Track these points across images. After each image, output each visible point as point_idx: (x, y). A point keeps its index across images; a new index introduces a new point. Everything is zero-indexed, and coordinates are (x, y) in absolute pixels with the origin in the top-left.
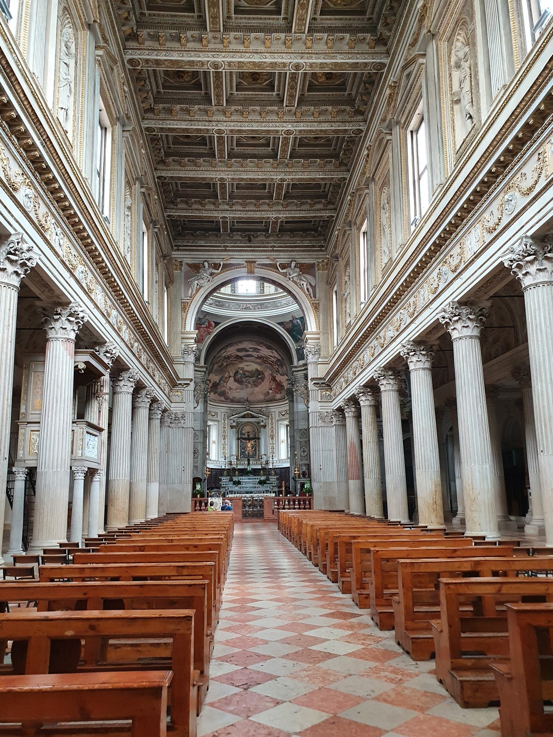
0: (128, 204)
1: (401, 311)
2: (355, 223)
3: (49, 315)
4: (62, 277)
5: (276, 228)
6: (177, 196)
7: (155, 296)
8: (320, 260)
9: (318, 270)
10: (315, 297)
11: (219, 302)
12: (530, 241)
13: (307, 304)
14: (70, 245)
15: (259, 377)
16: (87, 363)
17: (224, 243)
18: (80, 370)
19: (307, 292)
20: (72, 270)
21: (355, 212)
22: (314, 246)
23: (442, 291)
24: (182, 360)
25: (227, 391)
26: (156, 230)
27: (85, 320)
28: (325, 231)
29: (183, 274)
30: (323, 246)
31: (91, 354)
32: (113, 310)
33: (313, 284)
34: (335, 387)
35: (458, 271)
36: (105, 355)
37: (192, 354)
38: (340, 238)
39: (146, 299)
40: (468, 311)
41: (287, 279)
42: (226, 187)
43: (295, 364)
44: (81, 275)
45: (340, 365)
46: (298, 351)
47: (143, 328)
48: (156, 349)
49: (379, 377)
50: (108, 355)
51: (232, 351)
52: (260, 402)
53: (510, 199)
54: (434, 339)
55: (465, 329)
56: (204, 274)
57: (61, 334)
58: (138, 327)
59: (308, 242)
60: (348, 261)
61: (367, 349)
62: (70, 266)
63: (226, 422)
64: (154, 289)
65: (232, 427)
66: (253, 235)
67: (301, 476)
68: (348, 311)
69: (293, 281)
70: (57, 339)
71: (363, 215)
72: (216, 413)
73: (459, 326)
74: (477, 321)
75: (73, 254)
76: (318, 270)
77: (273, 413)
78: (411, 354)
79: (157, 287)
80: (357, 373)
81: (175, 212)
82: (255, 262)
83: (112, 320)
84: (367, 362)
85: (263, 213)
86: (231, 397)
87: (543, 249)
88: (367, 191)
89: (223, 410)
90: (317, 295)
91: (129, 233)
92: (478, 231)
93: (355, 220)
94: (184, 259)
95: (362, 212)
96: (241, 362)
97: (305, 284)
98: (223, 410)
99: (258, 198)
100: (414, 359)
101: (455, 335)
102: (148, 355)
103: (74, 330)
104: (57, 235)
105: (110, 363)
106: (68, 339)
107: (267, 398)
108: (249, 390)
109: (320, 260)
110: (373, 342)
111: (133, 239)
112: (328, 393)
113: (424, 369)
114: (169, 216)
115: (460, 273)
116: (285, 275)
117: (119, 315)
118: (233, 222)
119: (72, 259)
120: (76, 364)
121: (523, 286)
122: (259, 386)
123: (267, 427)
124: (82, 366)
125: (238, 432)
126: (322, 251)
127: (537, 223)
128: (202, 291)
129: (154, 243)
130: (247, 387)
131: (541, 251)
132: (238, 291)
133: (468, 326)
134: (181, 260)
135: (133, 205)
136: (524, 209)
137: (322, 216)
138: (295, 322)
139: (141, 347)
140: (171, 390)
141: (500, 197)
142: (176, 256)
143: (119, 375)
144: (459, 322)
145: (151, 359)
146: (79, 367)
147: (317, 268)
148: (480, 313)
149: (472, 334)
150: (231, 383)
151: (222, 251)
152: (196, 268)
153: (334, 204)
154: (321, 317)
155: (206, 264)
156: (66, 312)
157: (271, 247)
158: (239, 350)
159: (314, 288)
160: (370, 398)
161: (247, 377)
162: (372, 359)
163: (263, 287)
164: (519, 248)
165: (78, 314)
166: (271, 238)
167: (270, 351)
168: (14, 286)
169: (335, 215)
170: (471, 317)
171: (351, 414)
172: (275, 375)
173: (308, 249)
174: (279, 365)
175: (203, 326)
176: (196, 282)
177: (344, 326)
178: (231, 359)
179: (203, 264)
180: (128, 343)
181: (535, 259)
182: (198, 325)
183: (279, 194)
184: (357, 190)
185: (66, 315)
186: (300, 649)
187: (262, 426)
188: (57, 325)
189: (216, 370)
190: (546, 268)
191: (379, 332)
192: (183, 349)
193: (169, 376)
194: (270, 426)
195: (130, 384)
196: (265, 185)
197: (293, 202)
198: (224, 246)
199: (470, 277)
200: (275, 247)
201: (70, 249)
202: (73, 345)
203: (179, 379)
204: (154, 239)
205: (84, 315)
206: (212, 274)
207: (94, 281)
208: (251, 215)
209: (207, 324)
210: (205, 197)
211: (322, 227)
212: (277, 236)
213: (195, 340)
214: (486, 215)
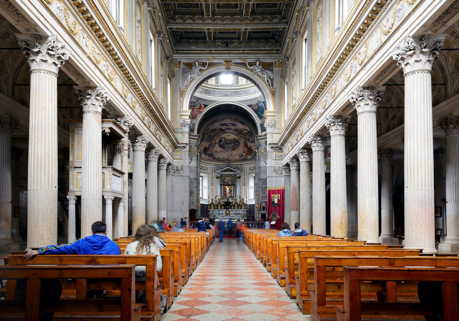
0: (139, 18)
1: (327, 95)
2: (300, 33)
3: (84, 95)
4: (90, 68)
5: (245, 37)
6: (175, 14)
7: (161, 85)
8: (277, 60)
9: (275, 67)
10: (273, 86)
11: (207, 90)
12: (412, 40)
13: (267, 91)
14: (94, 46)
15: (236, 143)
16: (111, 128)
17: (209, 48)
18: (106, 133)
19: (267, 83)
20: (97, 64)
21: (300, 24)
22: (272, 50)
23: (352, 79)
24: (180, 130)
26: (160, 38)
27: (108, 99)
28: (280, 39)
29: (181, 70)
30: (279, 50)
31: (113, 122)
32: (129, 94)
33: (272, 77)
34: (285, 150)
35: (363, 64)
36: (124, 124)
38: (290, 44)
39: (154, 87)
40: (369, 93)
41: (253, 73)
42: (209, 6)
44: (104, 67)
45: (287, 134)
47: (151, 106)
48: (161, 122)
49: (312, 141)
50: (126, 124)
51: (217, 125)
52: (236, 161)
53: (400, 8)
54: (347, 114)
55: (366, 106)
56: (196, 70)
57: (92, 108)
58: (148, 106)
59: (268, 47)
60: (295, 60)
61: (305, 122)
62: (95, 61)
63: (214, 174)
64: (160, 80)
65: (217, 178)
66: (230, 42)
68: (294, 96)
69: (257, 75)
70: (89, 112)
71: (305, 27)
72: (207, 168)
73: (362, 104)
74: (375, 100)
75: (97, 52)
76: (275, 67)
77: (245, 169)
78: (332, 124)
79: (162, 79)
80: (299, 140)
81: (174, 26)
82: (231, 61)
83: (129, 100)
84: (305, 131)
85: (236, 25)
86: (217, 158)
87: (421, 46)
88: (308, 8)
89: (212, 166)
90: (274, 85)
91: (140, 39)
92: (378, 34)
93: (300, 30)
94: (182, 60)
95: (304, 24)
96: (223, 133)
97: (266, 77)
98: (212, 166)
99: (232, 15)
100: (334, 128)
101: (359, 110)
102: (156, 126)
103: (101, 106)
104: (84, 38)
105: (128, 129)
106: (97, 112)
108: (229, 153)
109: (277, 60)
110: (309, 118)
111: (143, 44)
112: (280, 154)
113: (340, 135)
114: (170, 28)
115: (364, 66)
116: (252, 70)
117: (133, 97)
118: (216, 32)
119: (96, 56)
120: (104, 129)
121: (405, 73)
122: (236, 150)
123: (241, 178)
124: (107, 131)
125: (222, 181)
126: (278, 53)
127: (417, 25)
128: (194, 82)
129: (160, 47)
130: (228, 151)
131: (419, 47)
133: (368, 104)
134: (179, 60)
135: (142, 20)
136: (409, 15)
137: (278, 28)
138: (260, 104)
139: (150, 120)
140: (174, 151)
141: (394, 8)
142: (176, 58)
143: (136, 139)
144: (362, 101)
145: (158, 129)
146: (106, 131)
148: (377, 94)
149: (371, 110)
150: (217, 148)
151: (208, 53)
152: (190, 66)
153: (286, 19)
154: (277, 101)
155: (197, 63)
156: (94, 94)
157: (242, 50)
158: (222, 125)
159: (272, 80)
160: (306, 156)
162: (308, 129)
163: (238, 80)
164: (403, 46)
165: (103, 95)
166: (242, 44)
167: (243, 125)
168: (54, 73)
169: (287, 27)
170: (371, 97)
171: (294, 168)
173: (268, 52)
174: (249, 136)
175: (196, 107)
176: (190, 76)
177: (292, 107)
178: (216, 131)
179: (195, 63)
180: (141, 117)
181: (414, 53)
182: (192, 106)
183: (247, 12)
184: (302, 7)
185: (95, 95)
186: (230, 299)
188: (89, 102)
189: (206, 139)
190: (421, 60)
191: (313, 110)
192: (181, 123)
193: (172, 141)
194: (243, 177)
195: (143, 145)
196: (237, 4)
197: (257, 18)
198: (209, 50)
199: (371, 68)
200: (245, 50)
201: (94, 49)
202: (100, 117)
203: (178, 143)
204: (159, 44)
205: (107, 95)
206: (201, 70)
207: (114, 73)
208: (227, 27)
209: (199, 106)
210: (195, 14)
211: (278, 36)
212: (246, 42)
213: (190, 117)
214: (384, 22)
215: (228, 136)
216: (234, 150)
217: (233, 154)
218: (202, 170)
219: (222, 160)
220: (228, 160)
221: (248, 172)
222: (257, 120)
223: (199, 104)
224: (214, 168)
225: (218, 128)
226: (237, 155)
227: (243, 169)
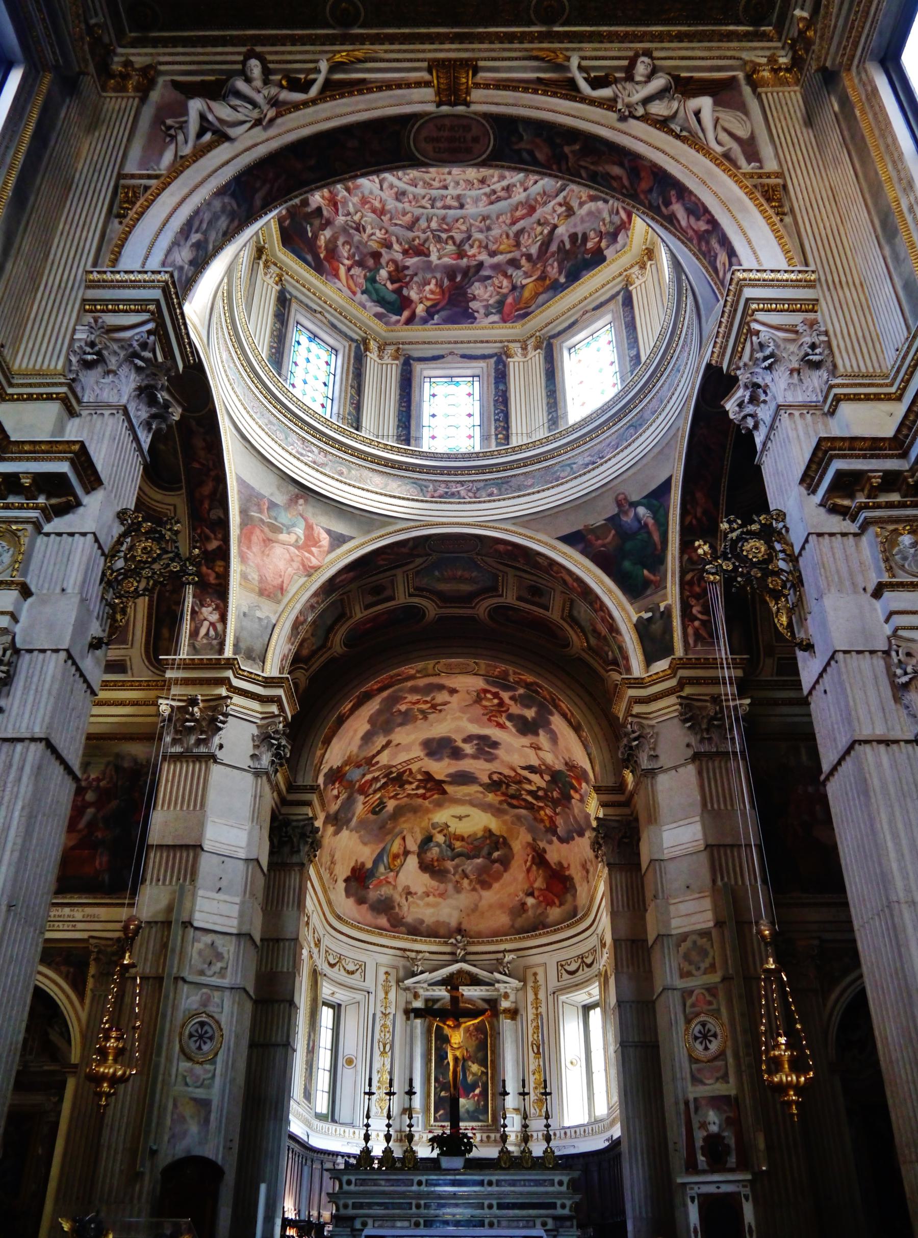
15: (496, 855)
25: (397, 898)
33: (743, 133)
37: (124, 371)
43: (637, 667)
46: (642, 628)
52: (497, 934)
63: (392, 995)
67: (701, 1158)
72: (362, 967)
77: (540, 971)
86: (409, 919)
96: (439, 805)
107: (519, 922)
108: (464, 899)
122: (496, 886)
130: (458, 889)
132: (419, 439)
138: (628, 519)
147: (747, 90)
161: (460, 855)
167: (526, 741)
172: (542, 844)
175: (283, 537)
187: (506, 1011)
189: (362, 823)
194: (531, 1012)
209: (300, 531)
215: (460, 818)
216: (486, 885)
217: (484, 904)
218: (336, 974)
219: (432, 933)
220: (459, 930)
221: (553, 983)
222: (620, 605)
223: (302, 524)
224: (396, 968)
225: (414, 767)
227: (530, 973)
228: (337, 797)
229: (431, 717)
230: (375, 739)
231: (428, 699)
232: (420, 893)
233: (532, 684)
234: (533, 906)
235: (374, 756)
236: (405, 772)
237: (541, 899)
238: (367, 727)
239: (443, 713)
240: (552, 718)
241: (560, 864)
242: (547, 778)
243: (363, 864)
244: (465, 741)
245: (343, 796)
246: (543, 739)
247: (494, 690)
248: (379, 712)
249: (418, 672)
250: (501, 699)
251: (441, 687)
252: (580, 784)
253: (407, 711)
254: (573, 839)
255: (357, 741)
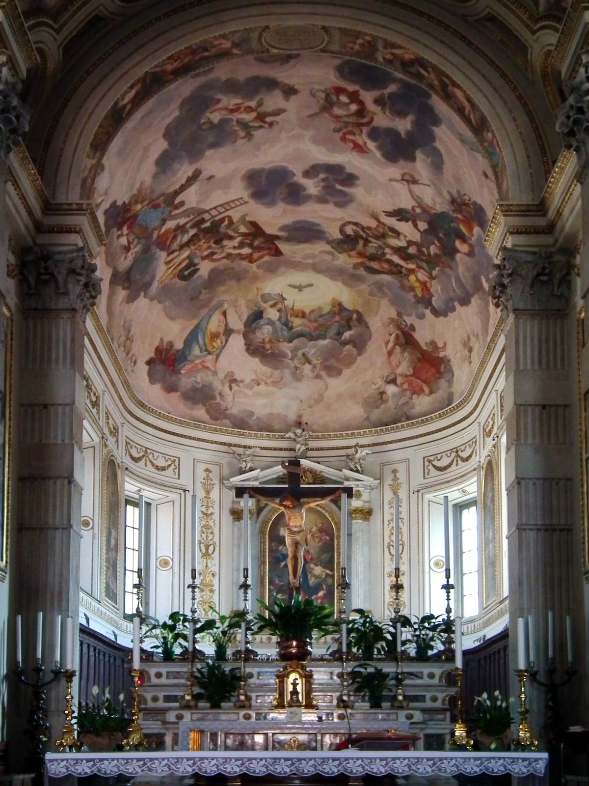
25: (218, 385)
86: (234, 411)
89: (206, 454)
107: (376, 414)
108: (307, 388)
122: (346, 372)
130: (297, 376)
167: (395, 171)
216: (333, 370)
219: (265, 427)
226: (353, 396)
228: (127, 249)
229: (257, 134)
230: (176, 166)
231: (253, 104)
232: (247, 381)
233: (412, 63)
234: (394, 395)
235: (177, 193)
236: (223, 220)
237: (406, 386)
238: (162, 145)
239: (276, 128)
240: (436, 130)
241: (433, 343)
242: (423, 226)
243: (171, 344)
244: (307, 174)
245: (136, 249)
246: (421, 166)
247: (351, 88)
248: (179, 123)
249: (235, 45)
250: (361, 103)
251: (271, 84)
252: (470, 230)
253: (223, 122)
254: (453, 309)
255: (149, 168)
